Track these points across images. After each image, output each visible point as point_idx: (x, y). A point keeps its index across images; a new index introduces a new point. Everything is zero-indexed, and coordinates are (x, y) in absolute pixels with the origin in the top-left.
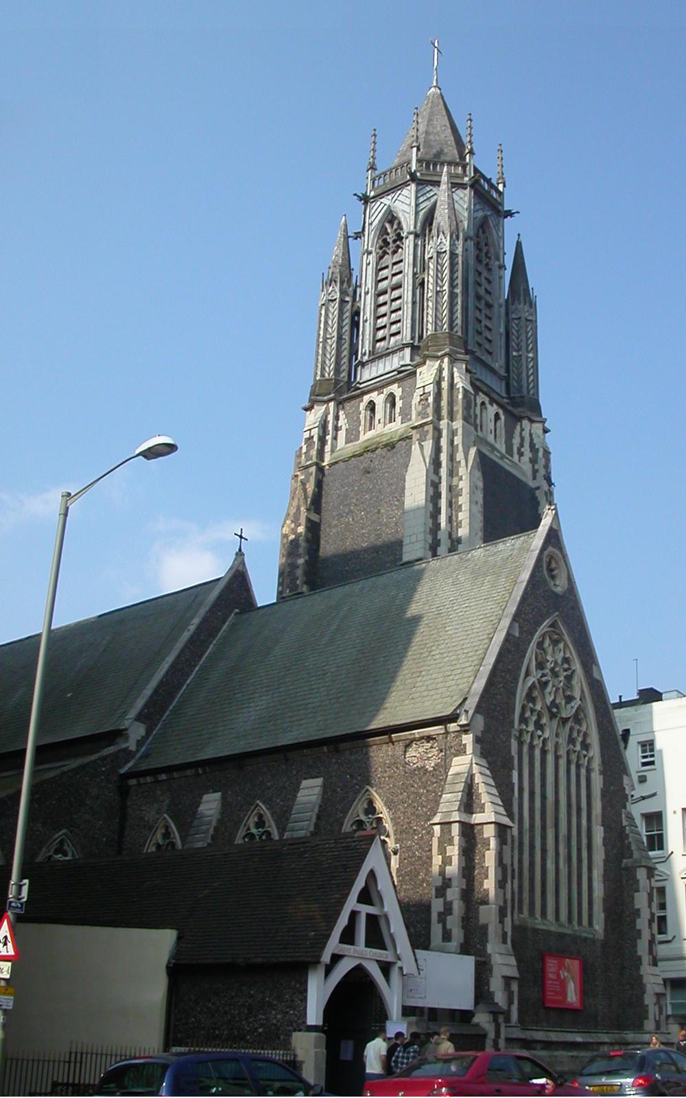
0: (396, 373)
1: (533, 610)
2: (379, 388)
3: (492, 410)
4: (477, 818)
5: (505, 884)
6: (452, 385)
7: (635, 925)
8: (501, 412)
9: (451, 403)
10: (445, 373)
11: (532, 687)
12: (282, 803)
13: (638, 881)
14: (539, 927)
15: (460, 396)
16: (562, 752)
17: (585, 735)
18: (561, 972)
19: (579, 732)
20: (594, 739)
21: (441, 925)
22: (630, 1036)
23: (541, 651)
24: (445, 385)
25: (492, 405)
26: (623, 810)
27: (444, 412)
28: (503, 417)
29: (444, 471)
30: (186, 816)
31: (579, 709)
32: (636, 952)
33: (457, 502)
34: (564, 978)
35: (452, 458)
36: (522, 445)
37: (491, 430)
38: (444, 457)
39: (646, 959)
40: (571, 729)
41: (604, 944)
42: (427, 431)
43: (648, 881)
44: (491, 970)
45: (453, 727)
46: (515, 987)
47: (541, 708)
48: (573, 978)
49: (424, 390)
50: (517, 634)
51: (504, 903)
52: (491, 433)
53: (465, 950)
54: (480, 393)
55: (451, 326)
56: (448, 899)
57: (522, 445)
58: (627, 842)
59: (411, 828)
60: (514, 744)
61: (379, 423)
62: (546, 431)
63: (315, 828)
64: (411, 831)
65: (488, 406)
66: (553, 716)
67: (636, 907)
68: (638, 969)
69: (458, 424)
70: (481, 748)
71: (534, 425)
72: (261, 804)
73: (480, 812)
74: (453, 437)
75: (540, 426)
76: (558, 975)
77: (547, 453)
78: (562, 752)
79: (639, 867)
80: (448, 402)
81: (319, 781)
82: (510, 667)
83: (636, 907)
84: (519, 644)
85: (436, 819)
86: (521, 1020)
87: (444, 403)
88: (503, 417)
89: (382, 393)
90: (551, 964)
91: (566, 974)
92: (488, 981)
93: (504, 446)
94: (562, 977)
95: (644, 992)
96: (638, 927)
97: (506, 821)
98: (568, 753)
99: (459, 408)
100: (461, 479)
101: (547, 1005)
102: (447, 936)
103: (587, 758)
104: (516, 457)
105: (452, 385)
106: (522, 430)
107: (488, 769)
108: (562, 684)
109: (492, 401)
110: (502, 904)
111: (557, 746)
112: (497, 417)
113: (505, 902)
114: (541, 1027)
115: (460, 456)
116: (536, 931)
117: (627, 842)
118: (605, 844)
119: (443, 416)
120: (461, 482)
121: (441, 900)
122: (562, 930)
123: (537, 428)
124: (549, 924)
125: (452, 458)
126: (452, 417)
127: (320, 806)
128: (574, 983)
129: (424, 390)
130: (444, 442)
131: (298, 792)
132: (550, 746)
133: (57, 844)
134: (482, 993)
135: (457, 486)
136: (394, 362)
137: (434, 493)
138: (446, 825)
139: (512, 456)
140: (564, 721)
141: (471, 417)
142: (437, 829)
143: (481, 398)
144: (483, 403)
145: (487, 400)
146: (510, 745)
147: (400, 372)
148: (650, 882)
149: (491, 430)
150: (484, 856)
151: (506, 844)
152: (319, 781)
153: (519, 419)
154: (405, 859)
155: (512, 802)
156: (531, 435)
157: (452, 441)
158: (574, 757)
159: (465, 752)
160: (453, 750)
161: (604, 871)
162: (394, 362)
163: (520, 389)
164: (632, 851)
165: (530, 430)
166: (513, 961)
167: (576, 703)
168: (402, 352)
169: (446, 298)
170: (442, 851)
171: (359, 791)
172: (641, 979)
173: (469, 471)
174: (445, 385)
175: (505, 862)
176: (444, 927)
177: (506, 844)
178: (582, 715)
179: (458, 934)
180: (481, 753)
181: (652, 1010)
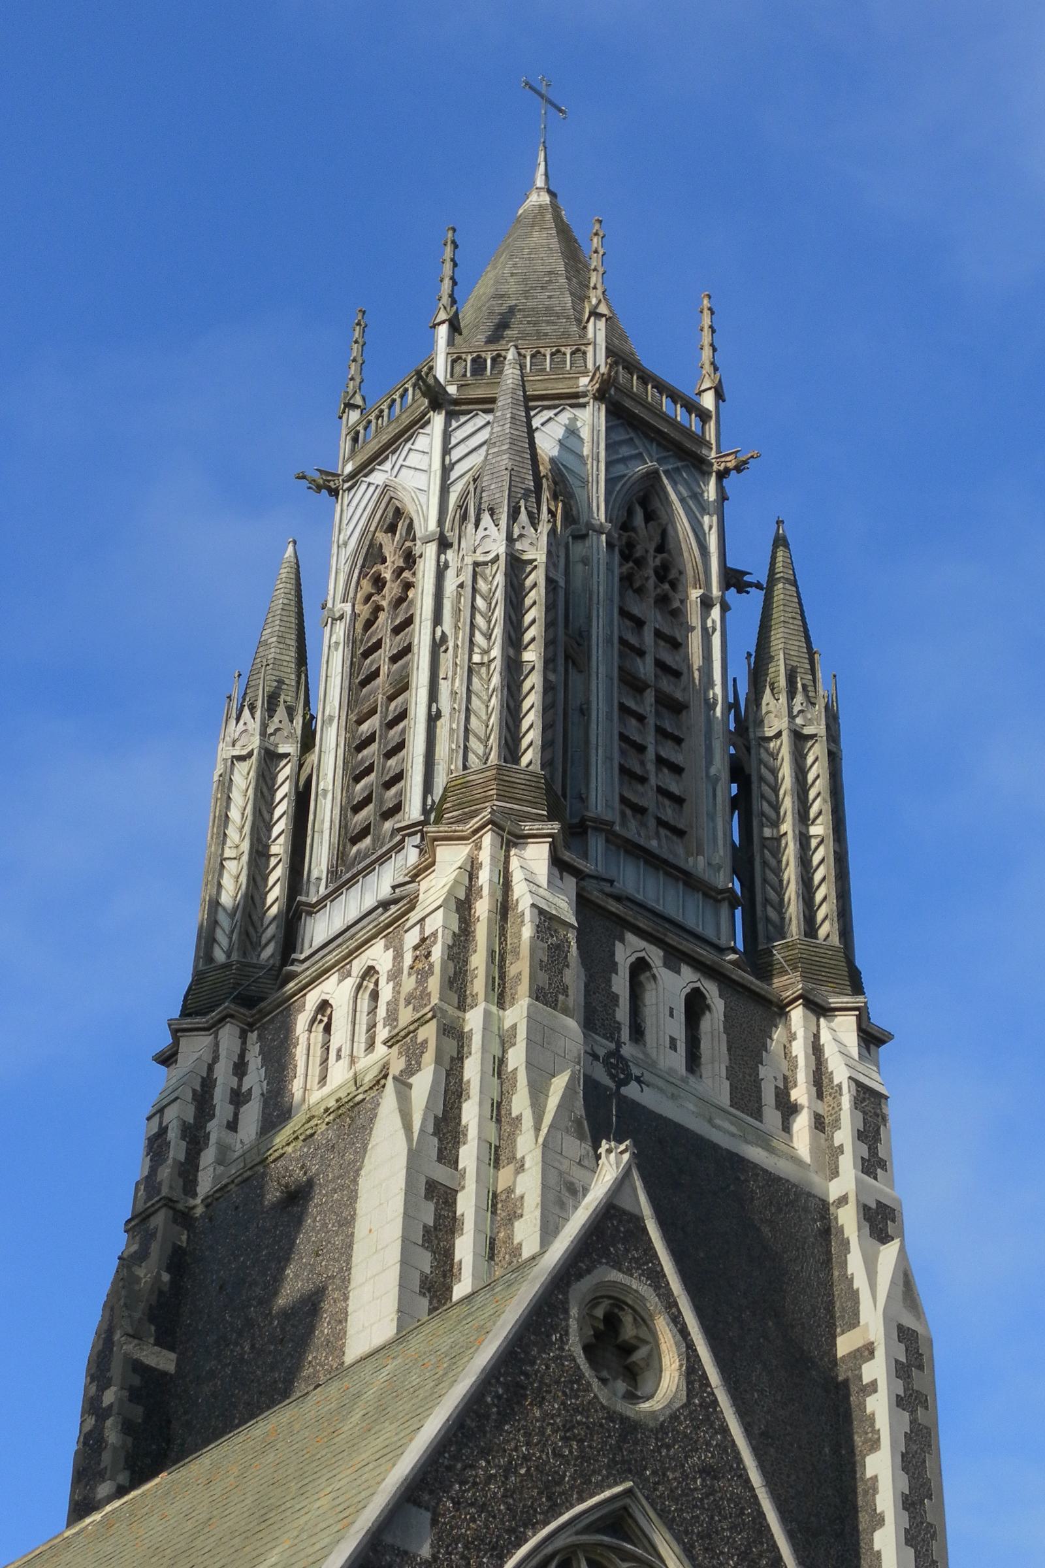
2: (342, 965)
6: (504, 908)
8: (711, 989)
9: (499, 959)
10: (484, 877)
15: (527, 932)
24: (482, 908)
25: (678, 972)
27: (478, 985)
29: (468, 1155)
33: (510, 1237)
35: (498, 1111)
37: (673, 1041)
38: (471, 1113)
42: (426, 1041)
49: (422, 930)
54: (630, 937)
55: (511, 747)
61: (339, 1057)
65: (664, 974)
69: (517, 1014)
74: (504, 1051)
80: (491, 953)
87: (478, 961)
88: (717, 1005)
89: (349, 975)
99: (520, 967)
100: (521, 1168)
105: (504, 908)
109: (675, 958)
112: (695, 1005)
115: (520, 1103)
119: (474, 996)
120: (520, 1178)
125: (498, 1111)
126: (500, 994)
129: (422, 930)
130: (472, 1070)
135: (510, 1190)
137: (438, 1216)
139: (758, 1114)
144: (640, 967)
145: (655, 955)
149: (673, 1041)
156: (816, 1049)
157: (501, 1062)
168: (401, 856)
169: (496, 680)
173: (541, 1140)
174: (482, 908)
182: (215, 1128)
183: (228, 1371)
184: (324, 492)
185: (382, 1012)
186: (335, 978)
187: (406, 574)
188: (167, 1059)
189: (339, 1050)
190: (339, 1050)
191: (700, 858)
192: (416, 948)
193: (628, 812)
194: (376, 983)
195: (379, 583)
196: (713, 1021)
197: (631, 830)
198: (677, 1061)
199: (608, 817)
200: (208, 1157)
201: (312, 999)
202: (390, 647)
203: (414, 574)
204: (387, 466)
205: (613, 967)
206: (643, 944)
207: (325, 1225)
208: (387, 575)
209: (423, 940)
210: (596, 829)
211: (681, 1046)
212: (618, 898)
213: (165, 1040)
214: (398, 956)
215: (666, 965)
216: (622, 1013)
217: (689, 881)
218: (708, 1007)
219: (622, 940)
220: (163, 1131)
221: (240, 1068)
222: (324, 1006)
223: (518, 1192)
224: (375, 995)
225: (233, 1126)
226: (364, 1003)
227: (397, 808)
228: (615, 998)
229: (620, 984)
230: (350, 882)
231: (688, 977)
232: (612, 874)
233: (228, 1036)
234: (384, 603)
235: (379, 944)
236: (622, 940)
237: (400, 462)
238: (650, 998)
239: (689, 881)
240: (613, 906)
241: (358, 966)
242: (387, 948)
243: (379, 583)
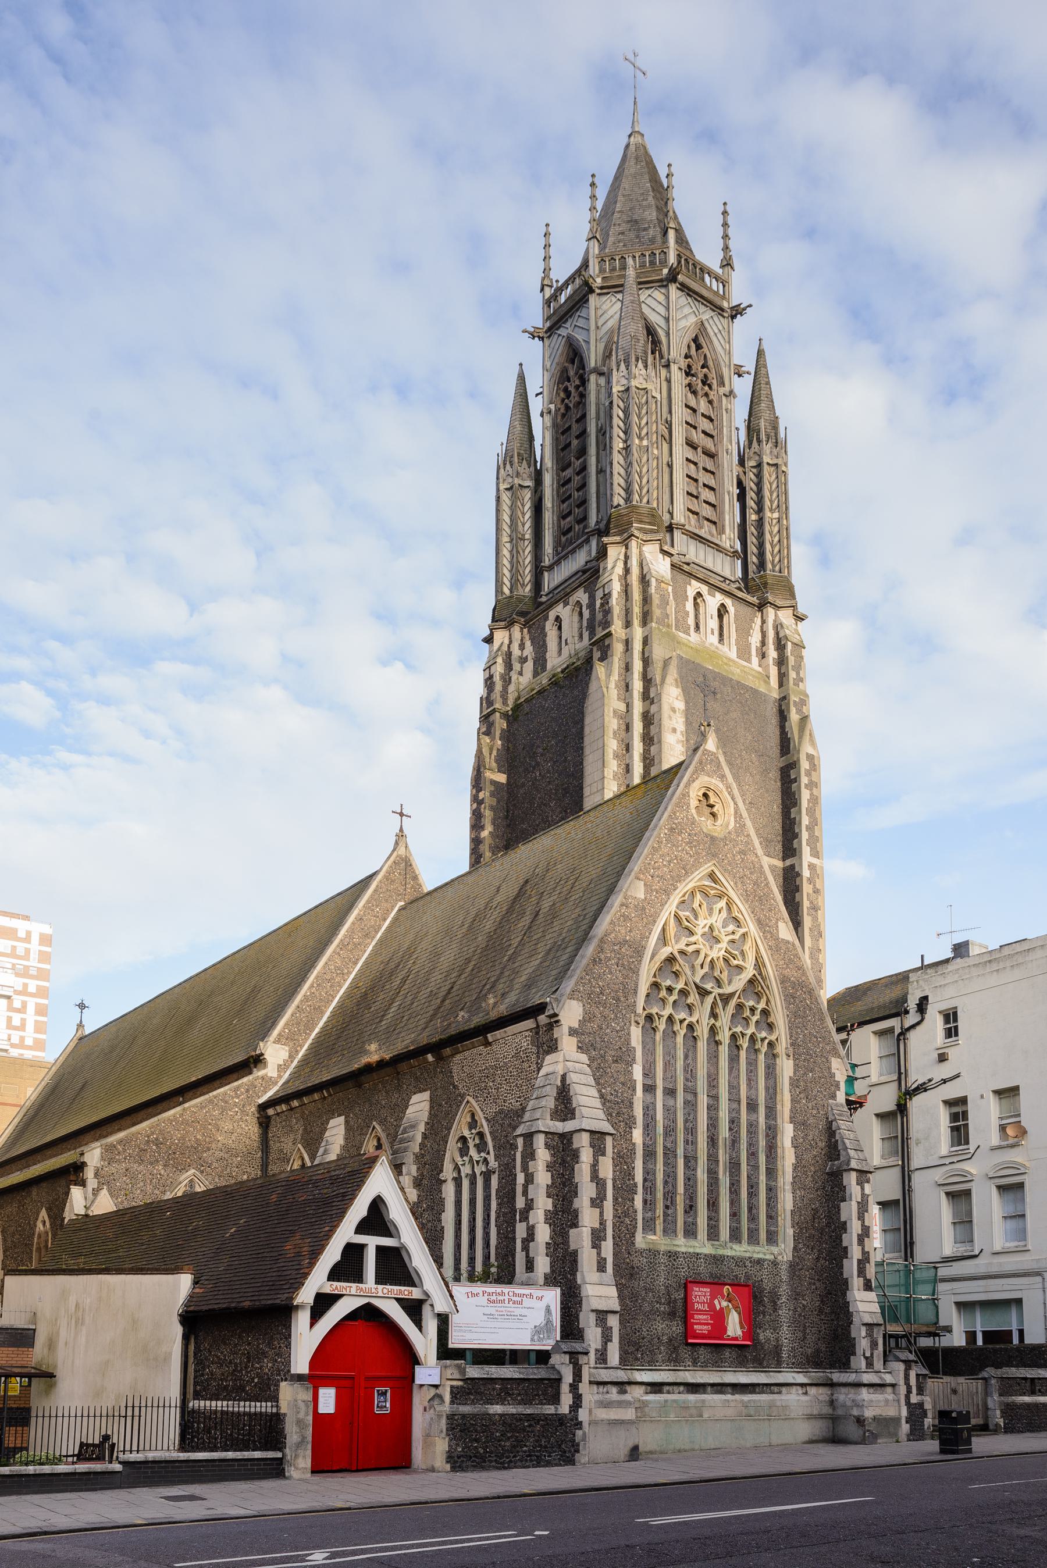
0: (581, 574)
1: (669, 862)
3: (713, 601)
4: (569, 1126)
5: (602, 1202)
7: (841, 1241)
8: (728, 602)
11: (671, 960)
12: (395, 1123)
13: (845, 1187)
14: (678, 1249)
16: (724, 1037)
17: (765, 1013)
18: (716, 1302)
19: (753, 1010)
20: (780, 1017)
21: (524, 1253)
22: (837, 1376)
23: (687, 914)
26: (830, 1101)
28: (731, 609)
30: (313, 1141)
31: (751, 982)
32: (842, 1274)
34: (721, 1309)
36: (763, 643)
39: (856, 1282)
40: (740, 1007)
41: (793, 1266)
43: (859, 1187)
44: (580, 1303)
45: (542, 1019)
46: (613, 1322)
47: (686, 984)
48: (736, 1308)
49: (604, 591)
50: (641, 895)
51: (601, 1224)
52: (713, 633)
53: (550, 1281)
54: (693, 582)
56: (531, 1223)
57: (763, 643)
58: (833, 1140)
59: (508, 1142)
60: (636, 1034)
62: (799, 618)
63: (421, 1149)
64: (508, 1146)
66: (703, 993)
67: (843, 1219)
68: (845, 1295)
70: (579, 1041)
71: (780, 613)
72: (377, 1126)
73: (571, 1119)
75: (790, 611)
76: (712, 1305)
77: (799, 646)
78: (724, 1037)
79: (845, 1170)
81: (426, 1095)
82: (628, 938)
83: (843, 1219)
84: (644, 909)
85: (519, 1131)
86: (623, 1361)
90: (700, 1295)
91: (724, 1304)
92: (578, 1315)
93: (734, 648)
94: (718, 1307)
95: (851, 1323)
96: (844, 1244)
97: (606, 1127)
98: (734, 1037)
101: (690, 1341)
102: (530, 1266)
103: (767, 1041)
104: (755, 660)
106: (763, 622)
107: (589, 1066)
108: (723, 952)
110: (597, 1225)
111: (713, 1030)
112: (722, 611)
113: (602, 1223)
114: (685, 1366)
116: (672, 1255)
117: (833, 1140)
118: (795, 1147)
120: (652, 706)
121: (524, 1224)
122: (721, 1252)
123: (786, 617)
124: (702, 1246)
127: (427, 1123)
128: (739, 1314)
129: (604, 591)
131: (407, 1108)
132: (703, 1032)
133: (186, 1186)
134: (571, 1329)
136: (580, 559)
138: (529, 1137)
140: (726, 999)
141: (667, 616)
142: (520, 1142)
143: (694, 587)
144: (699, 594)
145: (704, 589)
146: (629, 1034)
147: (584, 572)
148: (863, 1189)
150: (573, 1170)
151: (604, 1154)
152: (426, 1095)
153: (761, 607)
154: (503, 1178)
155: (632, 1103)
158: (745, 1044)
159: (557, 1048)
160: (545, 1047)
161: (794, 1178)
162: (580, 559)
163: (762, 565)
164: (839, 1151)
165: (775, 621)
166: (613, 1292)
167: (750, 972)
170: (525, 1168)
171: (461, 1102)
172: (848, 1307)
175: (601, 1175)
176: (527, 1256)
177: (604, 1154)
178: (760, 988)
179: (543, 1265)
180: (579, 1047)
181: (863, 1344)
182: (514, 676)
183: (530, 783)
184: (536, 339)
185: (585, 624)
186: (562, 605)
187: (581, 389)
188: (489, 640)
189: (566, 640)
190: (566, 640)
191: (724, 536)
192: (601, 599)
193: (690, 514)
194: (581, 608)
195: (568, 394)
196: (730, 618)
197: (692, 525)
198: (714, 639)
199: (682, 521)
200: (511, 688)
201: (552, 615)
202: (576, 429)
203: (585, 389)
204: (568, 325)
205: (686, 598)
206: (699, 585)
207: (567, 723)
208: (571, 389)
209: (605, 595)
210: (677, 528)
211: (716, 633)
212: (688, 564)
213: (487, 632)
214: (592, 598)
215: (709, 594)
216: (691, 621)
217: (718, 548)
218: (727, 611)
219: (690, 584)
220: (491, 677)
221: (522, 647)
222: (558, 619)
223: (652, 712)
224: (581, 614)
225: (521, 674)
226: (576, 618)
227: (584, 519)
228: (687, 613)
229: (690, 606)
230: (565, 557)
231: (719, 598)
232: (684, 551)
233: (516, 630)
234: (571, 405)
235: (581, 590)
236: (690, 584)
237: (575, 323)
238: (701, 610)
239: (718, 548)
240: (685, 567)
241: (573, 599)
242: (585, 593)
243: (568, 394)
